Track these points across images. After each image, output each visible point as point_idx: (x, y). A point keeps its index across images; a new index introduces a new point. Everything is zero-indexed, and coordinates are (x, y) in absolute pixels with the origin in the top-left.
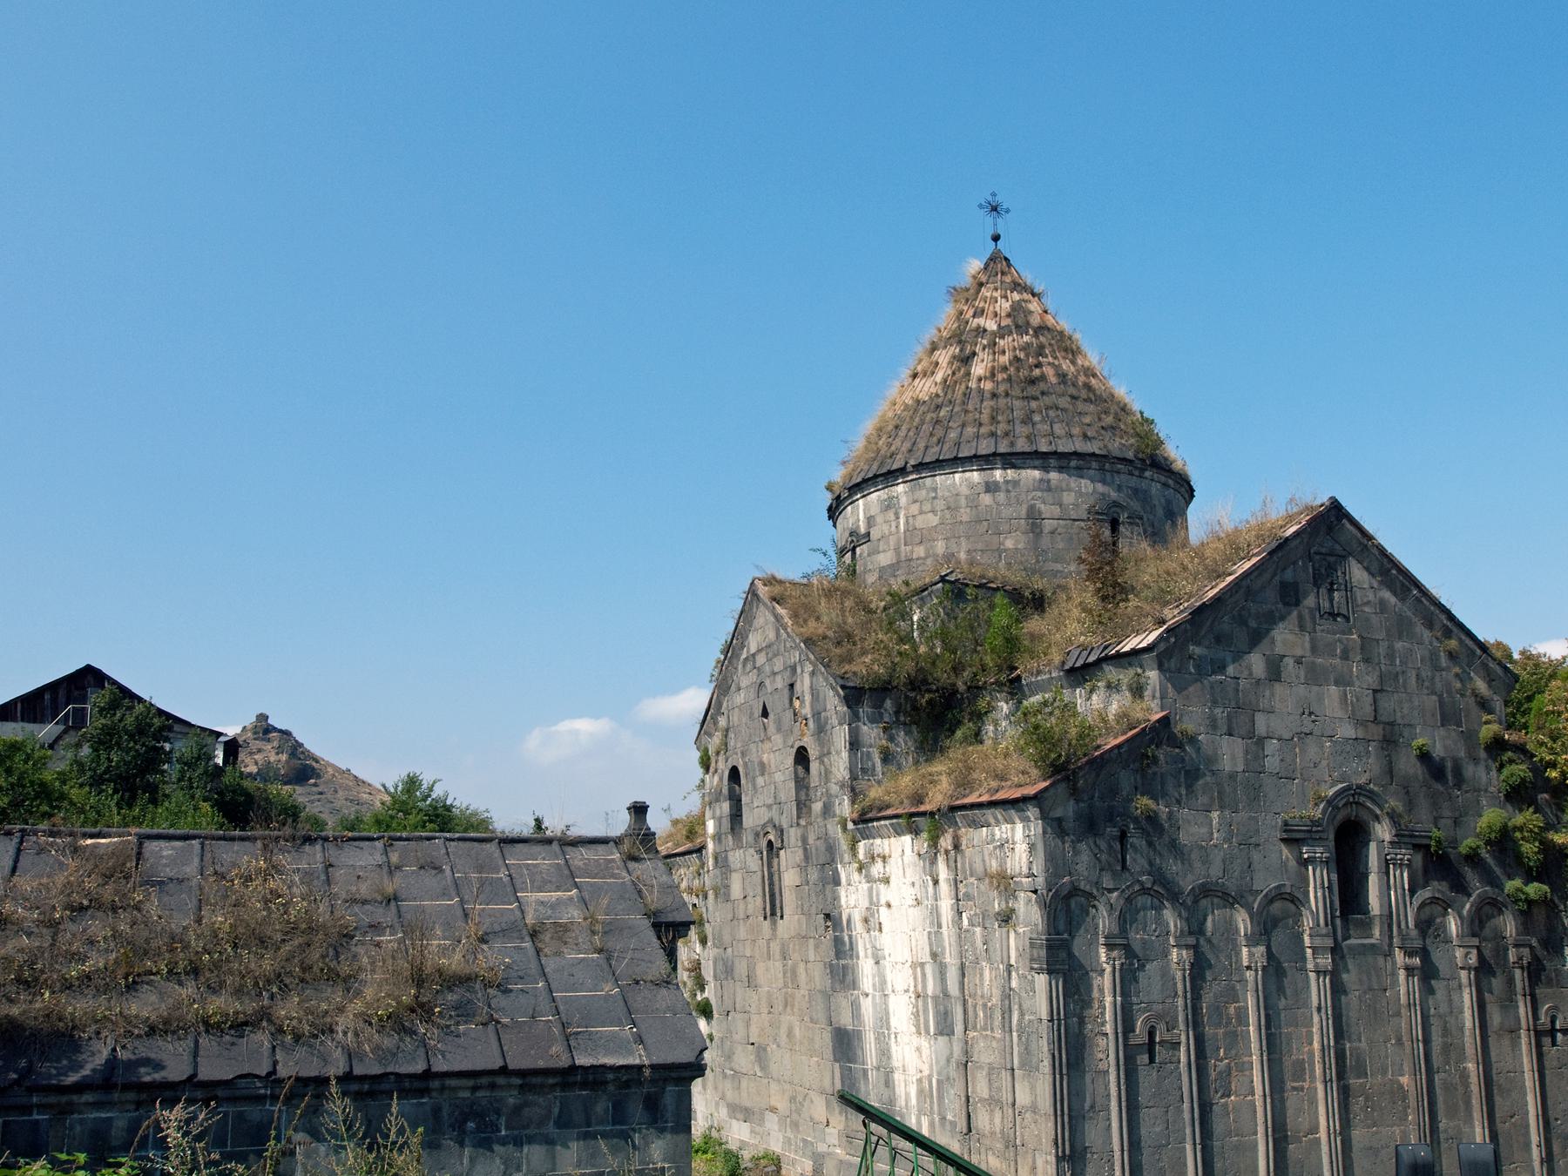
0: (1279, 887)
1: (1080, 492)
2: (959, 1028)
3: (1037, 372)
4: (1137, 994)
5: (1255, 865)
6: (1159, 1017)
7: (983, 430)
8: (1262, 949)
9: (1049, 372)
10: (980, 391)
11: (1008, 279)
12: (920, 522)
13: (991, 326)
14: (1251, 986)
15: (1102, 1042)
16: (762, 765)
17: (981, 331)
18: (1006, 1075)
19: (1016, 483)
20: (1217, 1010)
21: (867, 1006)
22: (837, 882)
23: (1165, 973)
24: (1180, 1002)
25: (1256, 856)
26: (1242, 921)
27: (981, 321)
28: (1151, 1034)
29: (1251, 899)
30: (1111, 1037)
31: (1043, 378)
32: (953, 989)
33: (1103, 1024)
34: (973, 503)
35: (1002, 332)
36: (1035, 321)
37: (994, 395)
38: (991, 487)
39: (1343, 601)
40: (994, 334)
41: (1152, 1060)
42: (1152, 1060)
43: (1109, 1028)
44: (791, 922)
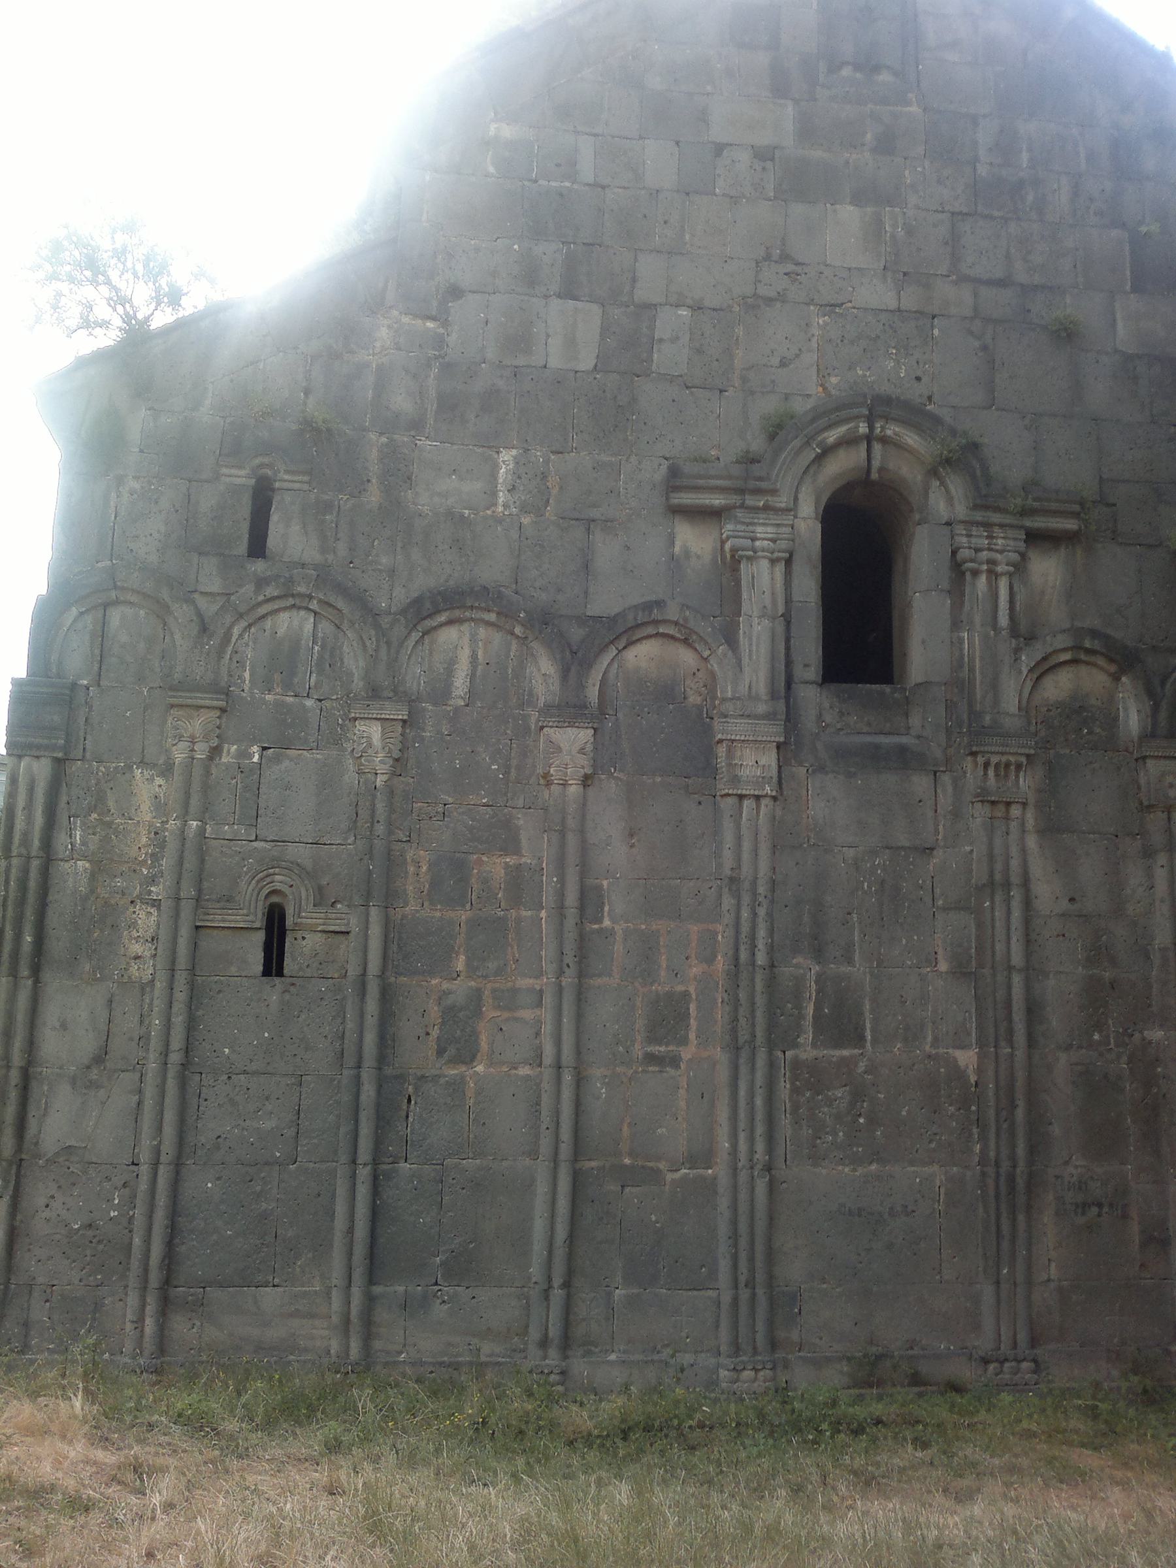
0: (648, 606)
8: (584, 735)
25: (607, 551)
33: (153, 881)
41: (273, 964)
42: (273, 964)
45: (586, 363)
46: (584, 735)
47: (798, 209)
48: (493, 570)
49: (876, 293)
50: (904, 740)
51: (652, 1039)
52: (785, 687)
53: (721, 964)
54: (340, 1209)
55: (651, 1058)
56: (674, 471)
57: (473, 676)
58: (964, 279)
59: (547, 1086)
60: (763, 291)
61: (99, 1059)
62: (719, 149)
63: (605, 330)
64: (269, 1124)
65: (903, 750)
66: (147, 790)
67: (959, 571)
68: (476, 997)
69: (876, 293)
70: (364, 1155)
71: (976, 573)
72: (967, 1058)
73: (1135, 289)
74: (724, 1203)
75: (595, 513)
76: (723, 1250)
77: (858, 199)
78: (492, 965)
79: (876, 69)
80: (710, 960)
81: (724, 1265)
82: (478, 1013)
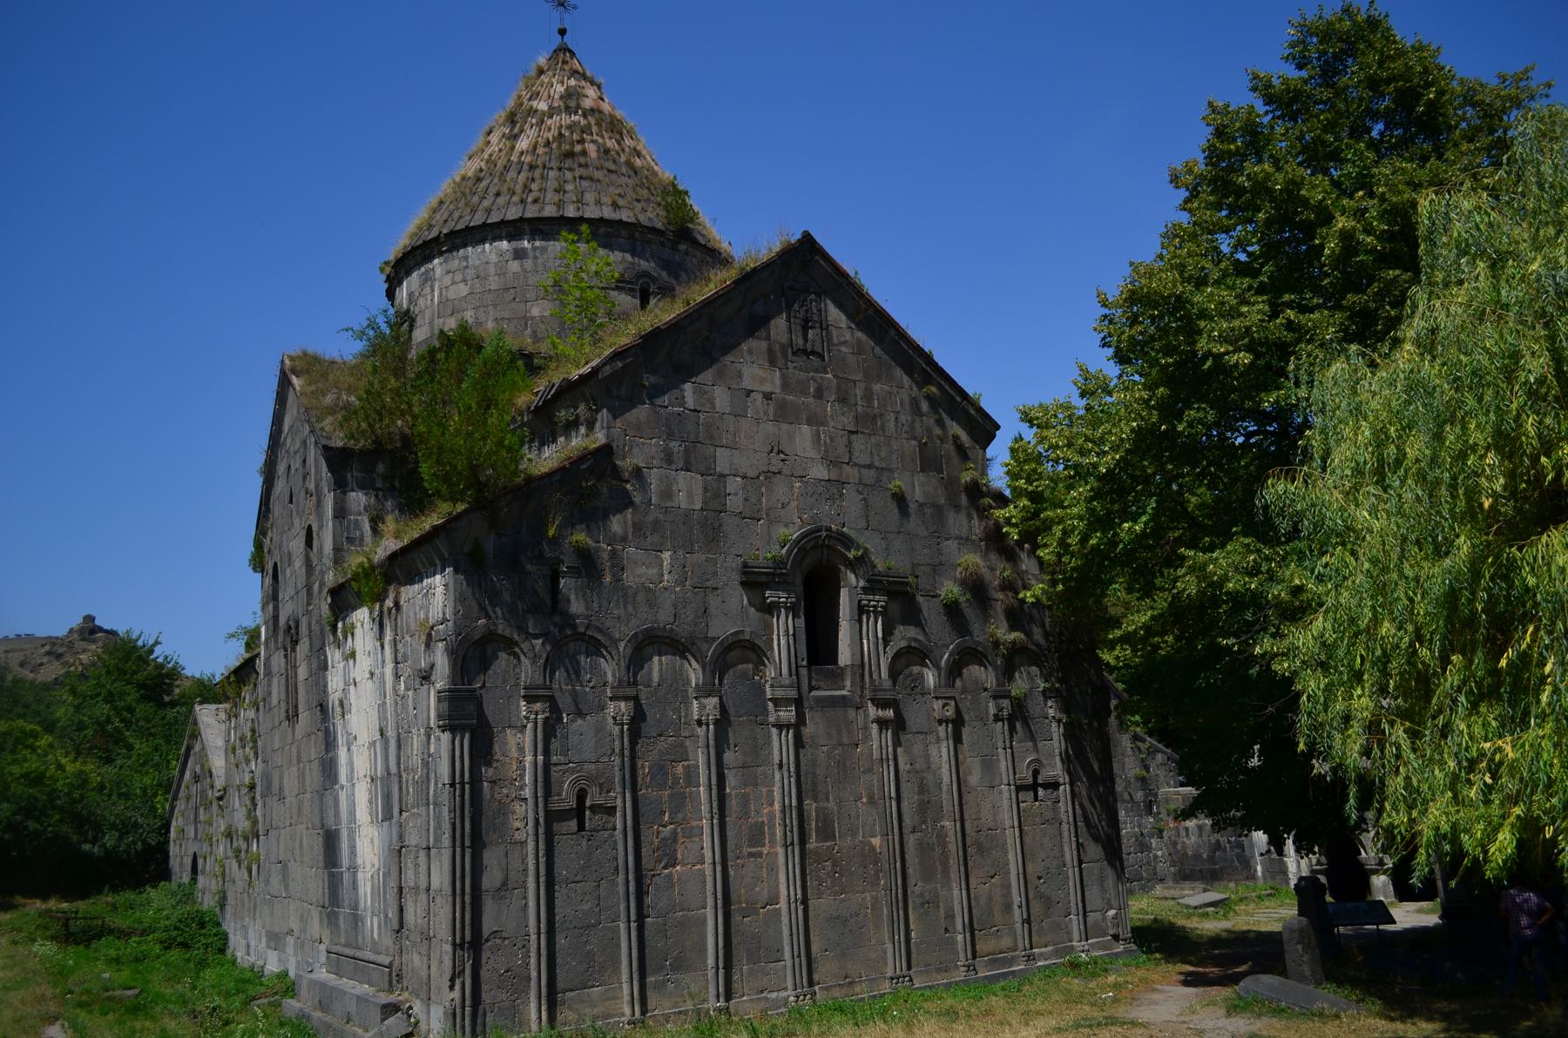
0: (737, 633)
1: (613, 262)
2: (396, 810)
3: (578, 148)
4: (565, 752)
5: (712, 611)
6: (591, 779)
7: (516, 199)
8: (715, 700)
9: (592, 149)
10: (521, 164)
11: (567, 68)
12: (451, 294)
13: (542, 106)
14: (702, 740)
15: (519, 809)
16: (289, 554)
17: (532, 112)
18: (422, 854)
19: (544, 249)
20: (661, 770)
21: (343, 796)
22: (326, 668)
23: (600, 729)
24: (617, 761)
25: (714, 602)
26: (694, 673)
27: (535, 104)
28: (581, 796)
29: (704, 646)
30: (531, 802)
31: (584, 153)
32: (393, 769)
33: (522, 788)
34: (502, 274)
35: (551, 112)
36: (587, 103)
37: (532, 167)
38: (519, 255)
39: (818, 339)
40: (544, 114)
41: (581, 827)
42: (581, 827)
43: (527, 792)
44: (304, 716)
45: (698, 507)
46: (715, 700)
47: (785, 426)
48: (664, 616)
49: (819, 472)
50: (844, 693)
51: (750, 846)
52: (795, 671)
53: (777, 806)
54: (624, 945)
55: (751, 855)
56: (745, 565)
57: (661, 670)
58: (856, 464)
59: (708, 872)
60: (773, 469)
61: (505, 883)
62: (749, 393)
63: (706, 489)
64: (586, 907)
65: (844, 697)
66: (512, 739)
67: (861, 610)
68: (674, 833)
69: (819, 472)
70: (633, 917)
71: (868, 612)
72: (876, 841)
73: (922, 470)
74: (785, 920)
75: (708, 584)
76: (786, 941)
77: (809, 423)
78: (680, 816)
79: (813, 353)
80: (772, 804)
81: (787, 949)
82: (675, 841)
